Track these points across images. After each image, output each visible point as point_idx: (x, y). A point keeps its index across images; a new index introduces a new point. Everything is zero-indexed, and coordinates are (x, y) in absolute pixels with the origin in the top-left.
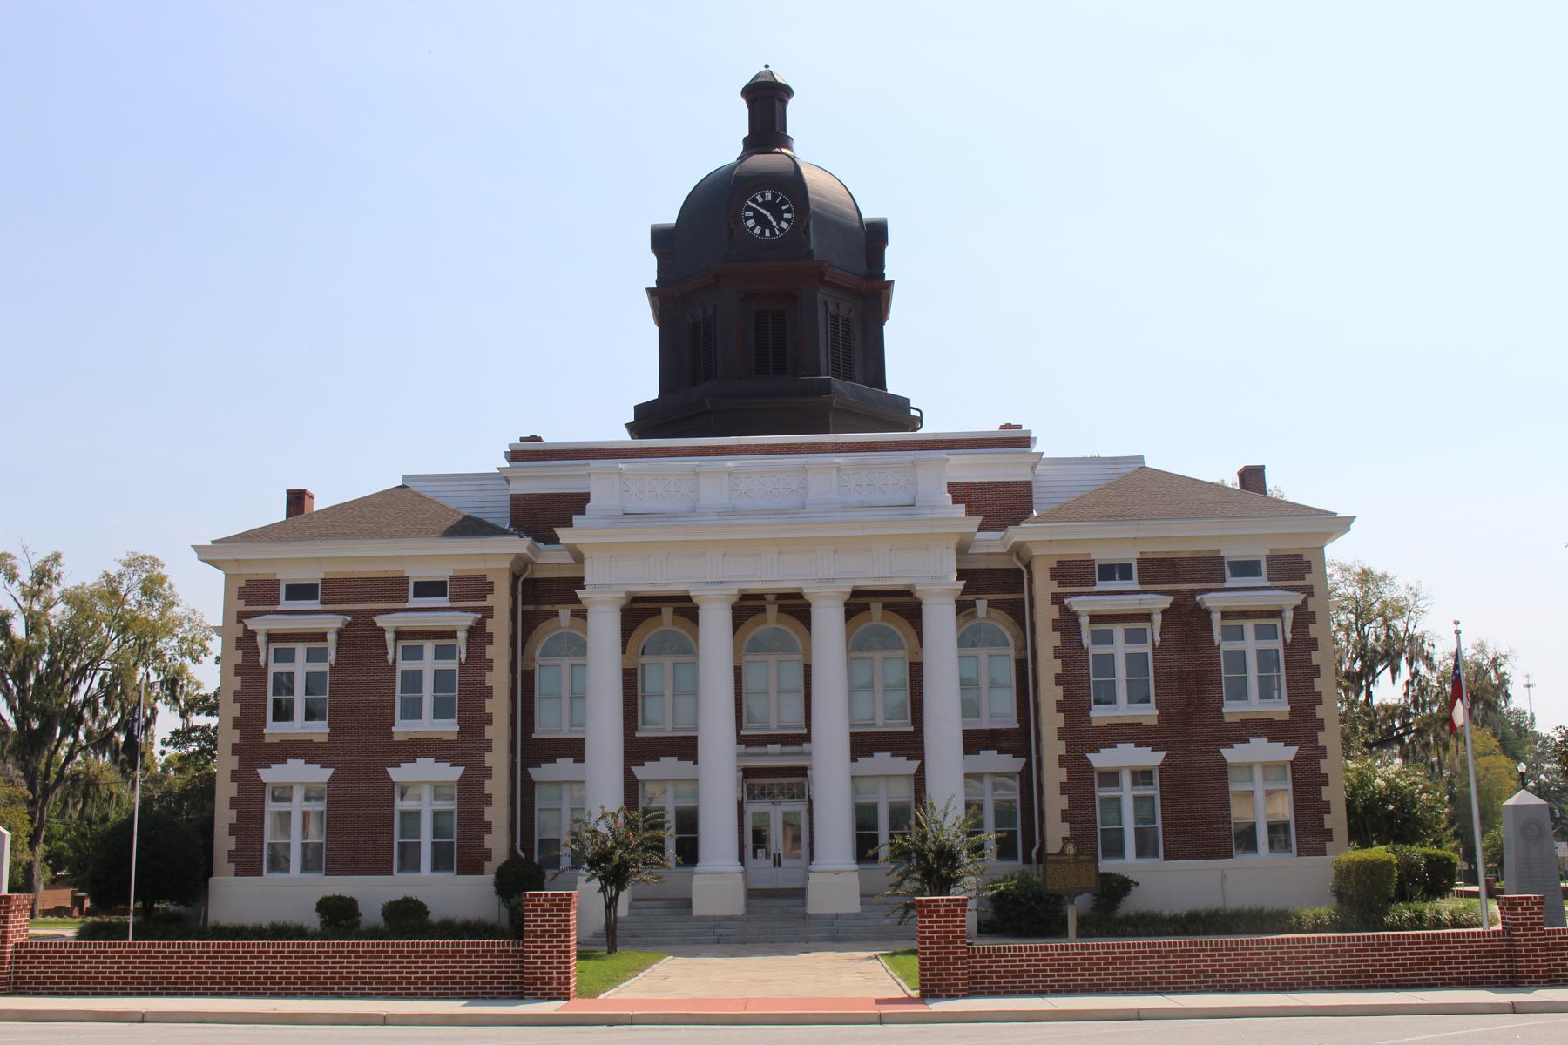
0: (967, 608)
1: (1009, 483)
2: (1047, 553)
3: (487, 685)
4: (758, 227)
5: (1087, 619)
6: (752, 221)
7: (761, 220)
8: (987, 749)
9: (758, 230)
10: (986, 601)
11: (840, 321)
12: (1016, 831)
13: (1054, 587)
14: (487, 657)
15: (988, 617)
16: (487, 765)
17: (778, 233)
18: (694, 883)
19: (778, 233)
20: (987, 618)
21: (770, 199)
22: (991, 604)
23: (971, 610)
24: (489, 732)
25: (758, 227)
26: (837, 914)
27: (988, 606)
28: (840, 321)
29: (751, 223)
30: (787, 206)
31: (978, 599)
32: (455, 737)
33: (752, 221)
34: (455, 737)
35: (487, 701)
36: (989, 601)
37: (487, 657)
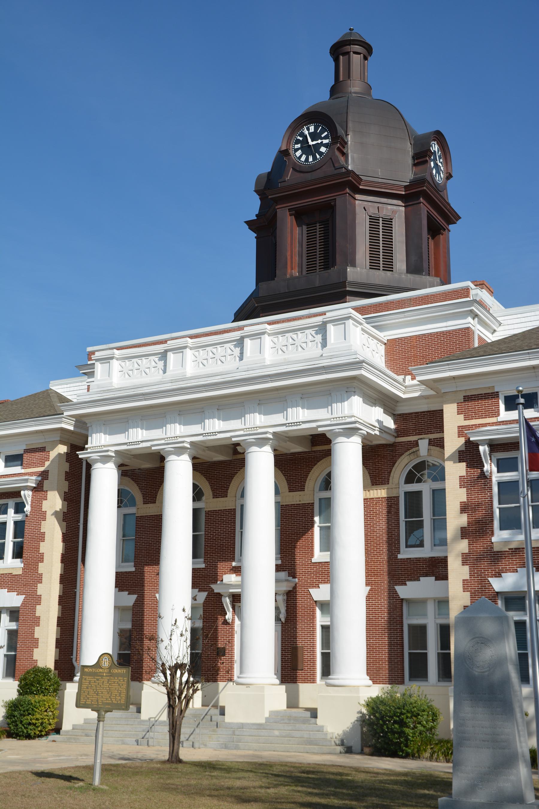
0: (412, 448)
1: (449, 332)
2: (455, 390)
3: (42, 531)
4: (304, 155)
5: (487, 448)
6: (300, 151)
7: (307, 149)
8: (426, 575)
9: (303, 158)
10: (426, 441)
11: (381, 222)
12: (450, 654)
13: (461, 421)
14: (43, 510)
15: (429, 455)
16: (38, 594)
17: (318, 156)
18: (143, 692)
19: (318, 156)
20: (428, 455)
21: (313, 131)
22: (432, 443)
23: (414, 449)
24: (42, 568)
25: (304, 155)
26: (242, 724)
27: (430, 444)
28: (381, 222)
29: (299, 153)
30: (326, 133)
31: (421, 439)
32: (20, 572)
33: (300, 151)
34: (20, 572)
35: (42, 544)
36: (430, 440)
37: (43, 510)
